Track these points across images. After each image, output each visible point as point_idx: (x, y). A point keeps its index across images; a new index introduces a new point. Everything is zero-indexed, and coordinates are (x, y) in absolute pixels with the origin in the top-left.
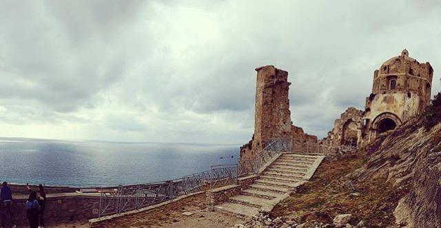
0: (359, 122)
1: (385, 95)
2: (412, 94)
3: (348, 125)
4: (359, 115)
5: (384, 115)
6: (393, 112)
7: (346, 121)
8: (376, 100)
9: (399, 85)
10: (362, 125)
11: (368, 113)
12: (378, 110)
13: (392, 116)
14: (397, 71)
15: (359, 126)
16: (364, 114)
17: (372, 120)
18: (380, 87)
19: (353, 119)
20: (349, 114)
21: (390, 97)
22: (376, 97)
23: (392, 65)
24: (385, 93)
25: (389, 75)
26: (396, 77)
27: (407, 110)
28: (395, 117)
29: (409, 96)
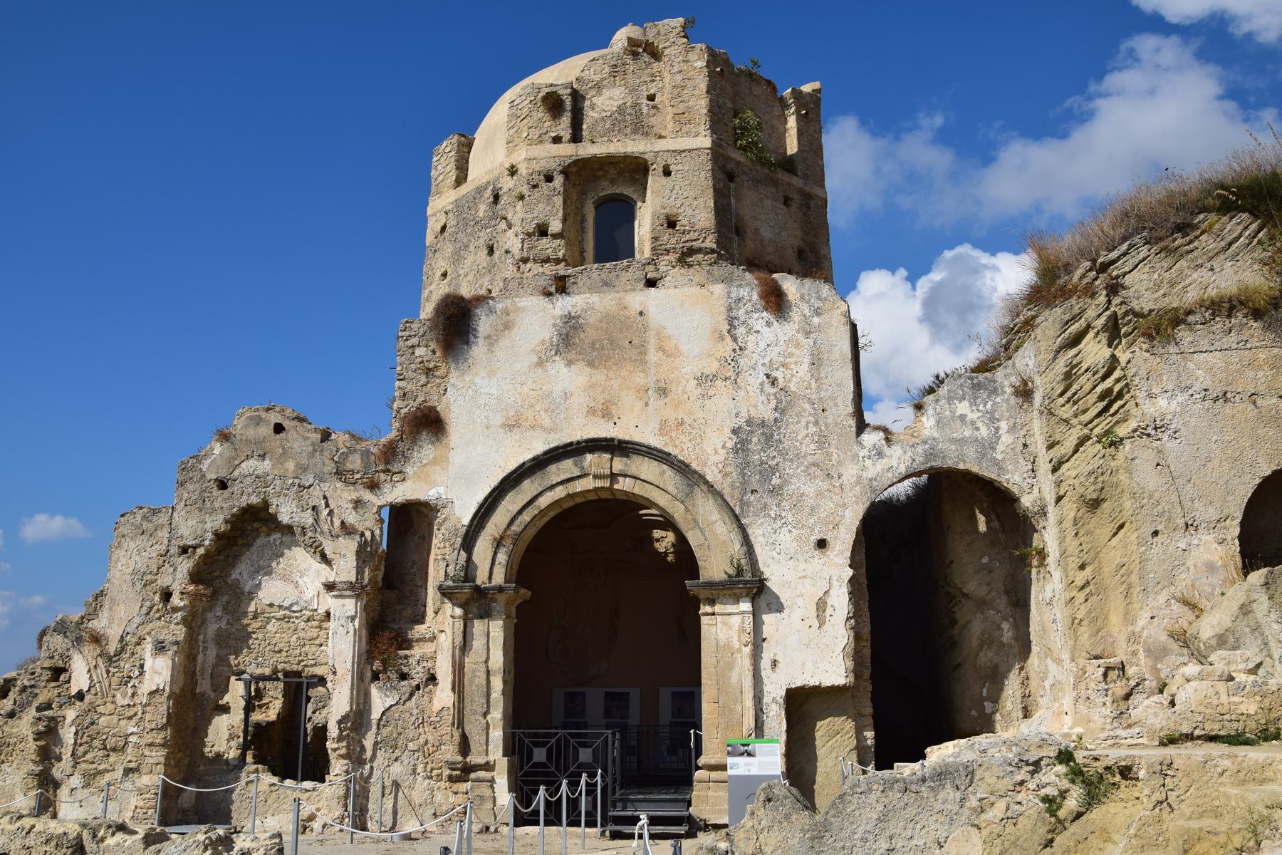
0: (347, 530)
1: (563, 304)
2: (790, 285)
3: (232, 560)
4: (340, 473)
5: (566, 468)
6: (653, 441)
7: (217, 522)
8: (491, 341)
9: (671, 224)
10: (365, 554)
11: (426, 451)
12: (511, 425)
13: (647, 468)
14: (640, 128)
15: (346, 569)
16: (391, 454)
17: (464, 513)
18: (512, 242)
19: (286, 511)
20: (250, 465)
21: (608, 318)
22: (484, 323)
23: (599, 87)
24: (561, 286)
25: (587, 150)
26: (636, 170)
27: (766, 412)
28: (670, 478)
29: (775, 301)
